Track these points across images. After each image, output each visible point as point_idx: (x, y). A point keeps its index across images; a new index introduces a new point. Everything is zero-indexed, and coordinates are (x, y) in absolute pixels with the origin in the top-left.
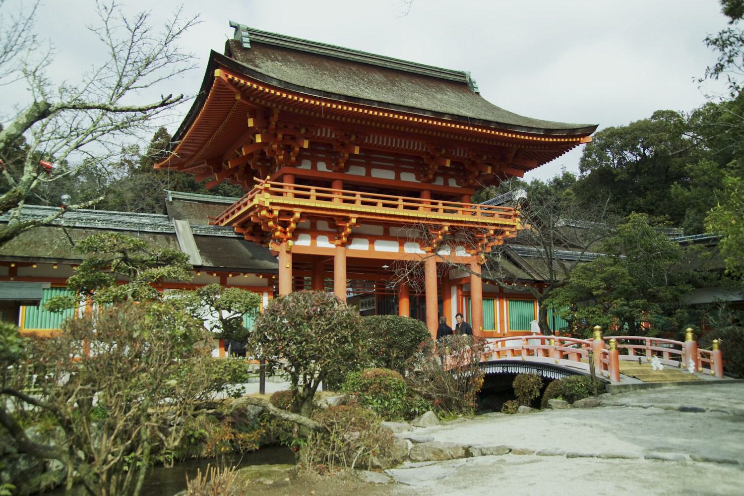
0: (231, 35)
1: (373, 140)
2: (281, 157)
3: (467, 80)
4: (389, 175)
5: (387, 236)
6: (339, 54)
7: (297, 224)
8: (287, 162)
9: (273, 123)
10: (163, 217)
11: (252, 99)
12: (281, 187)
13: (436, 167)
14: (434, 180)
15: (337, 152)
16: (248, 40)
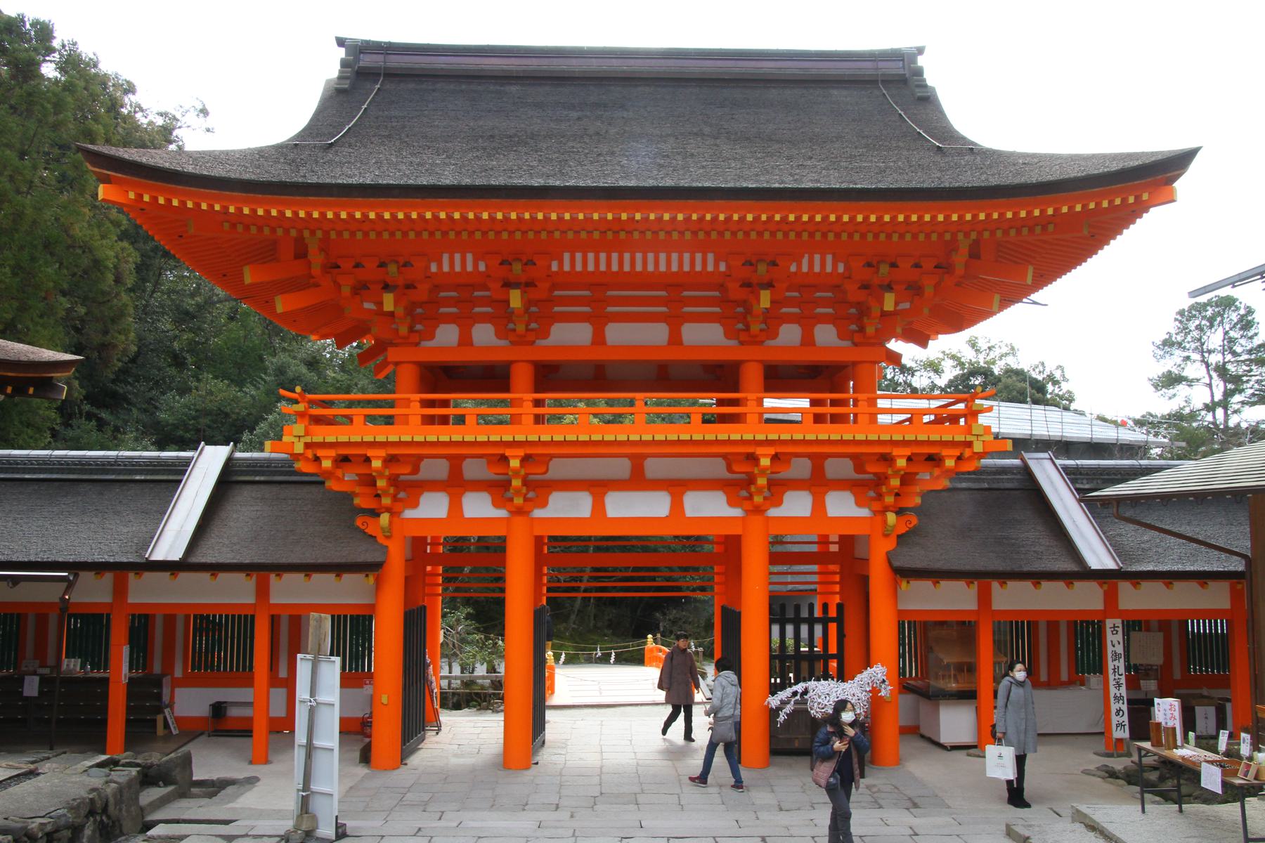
5: (638, 481)
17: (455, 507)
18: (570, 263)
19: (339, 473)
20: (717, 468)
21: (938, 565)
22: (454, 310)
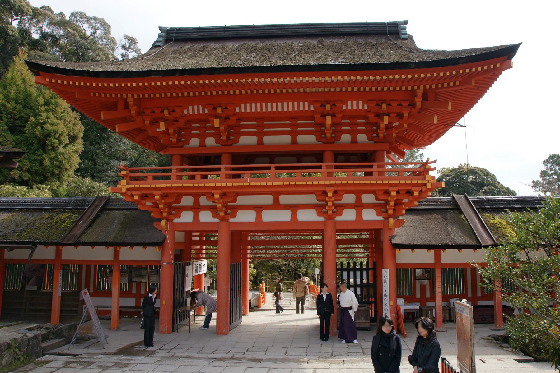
4: (286, 139)
5: (276, 205)
18: (245, 108)
19: (143, 202)
21: (416, 243)
22: (198, 132)
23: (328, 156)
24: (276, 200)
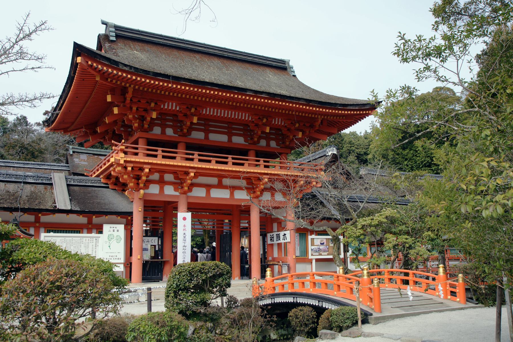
0: (102, 30)
1: (209, 111)
2: (136, 125)
3: (287, 65)
4: (223, 138)
5: (220, 186)
6: (187, 46)
7: (147, 177)
8: (141, 128)
9: (128, 99)
10: (65, 166)
11: (109, 80)
12: (137, 148)
13: (260, 133)
14: (258, 142)
15: (181, 121)
16: (114, 34)
17: (162, 189)
20: (243, 183)
23: (252, 153)
24: (220, 182)
